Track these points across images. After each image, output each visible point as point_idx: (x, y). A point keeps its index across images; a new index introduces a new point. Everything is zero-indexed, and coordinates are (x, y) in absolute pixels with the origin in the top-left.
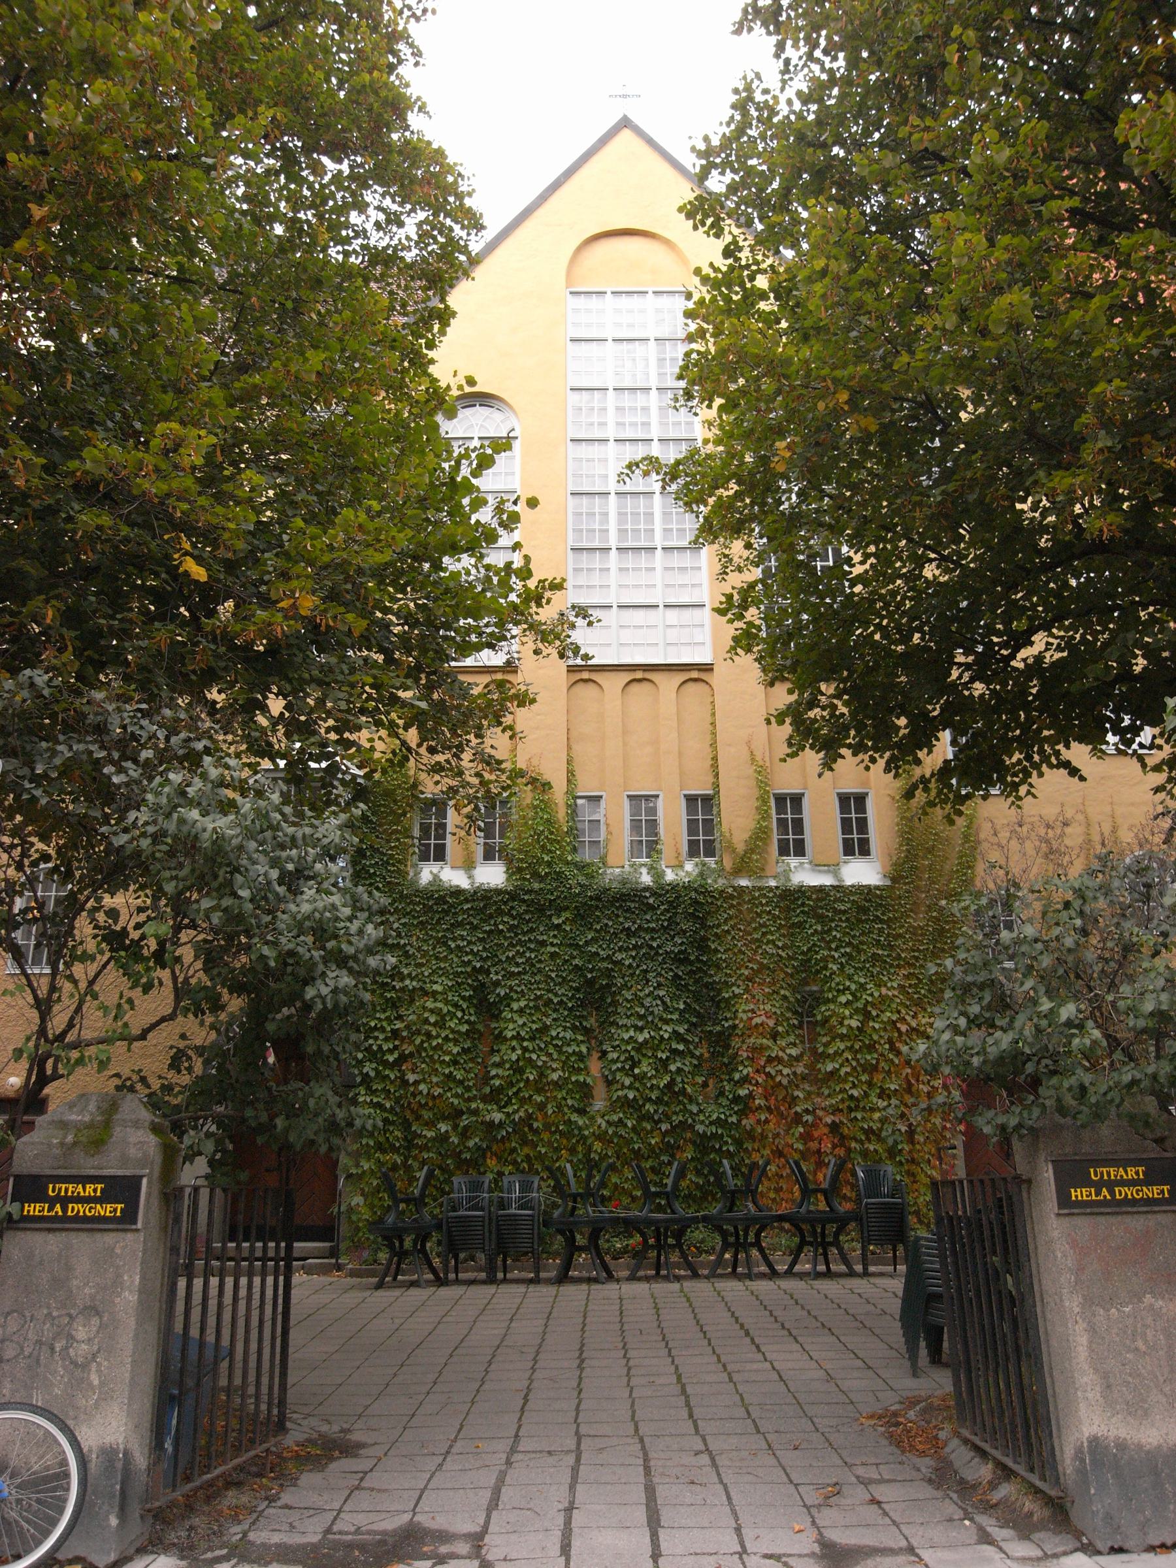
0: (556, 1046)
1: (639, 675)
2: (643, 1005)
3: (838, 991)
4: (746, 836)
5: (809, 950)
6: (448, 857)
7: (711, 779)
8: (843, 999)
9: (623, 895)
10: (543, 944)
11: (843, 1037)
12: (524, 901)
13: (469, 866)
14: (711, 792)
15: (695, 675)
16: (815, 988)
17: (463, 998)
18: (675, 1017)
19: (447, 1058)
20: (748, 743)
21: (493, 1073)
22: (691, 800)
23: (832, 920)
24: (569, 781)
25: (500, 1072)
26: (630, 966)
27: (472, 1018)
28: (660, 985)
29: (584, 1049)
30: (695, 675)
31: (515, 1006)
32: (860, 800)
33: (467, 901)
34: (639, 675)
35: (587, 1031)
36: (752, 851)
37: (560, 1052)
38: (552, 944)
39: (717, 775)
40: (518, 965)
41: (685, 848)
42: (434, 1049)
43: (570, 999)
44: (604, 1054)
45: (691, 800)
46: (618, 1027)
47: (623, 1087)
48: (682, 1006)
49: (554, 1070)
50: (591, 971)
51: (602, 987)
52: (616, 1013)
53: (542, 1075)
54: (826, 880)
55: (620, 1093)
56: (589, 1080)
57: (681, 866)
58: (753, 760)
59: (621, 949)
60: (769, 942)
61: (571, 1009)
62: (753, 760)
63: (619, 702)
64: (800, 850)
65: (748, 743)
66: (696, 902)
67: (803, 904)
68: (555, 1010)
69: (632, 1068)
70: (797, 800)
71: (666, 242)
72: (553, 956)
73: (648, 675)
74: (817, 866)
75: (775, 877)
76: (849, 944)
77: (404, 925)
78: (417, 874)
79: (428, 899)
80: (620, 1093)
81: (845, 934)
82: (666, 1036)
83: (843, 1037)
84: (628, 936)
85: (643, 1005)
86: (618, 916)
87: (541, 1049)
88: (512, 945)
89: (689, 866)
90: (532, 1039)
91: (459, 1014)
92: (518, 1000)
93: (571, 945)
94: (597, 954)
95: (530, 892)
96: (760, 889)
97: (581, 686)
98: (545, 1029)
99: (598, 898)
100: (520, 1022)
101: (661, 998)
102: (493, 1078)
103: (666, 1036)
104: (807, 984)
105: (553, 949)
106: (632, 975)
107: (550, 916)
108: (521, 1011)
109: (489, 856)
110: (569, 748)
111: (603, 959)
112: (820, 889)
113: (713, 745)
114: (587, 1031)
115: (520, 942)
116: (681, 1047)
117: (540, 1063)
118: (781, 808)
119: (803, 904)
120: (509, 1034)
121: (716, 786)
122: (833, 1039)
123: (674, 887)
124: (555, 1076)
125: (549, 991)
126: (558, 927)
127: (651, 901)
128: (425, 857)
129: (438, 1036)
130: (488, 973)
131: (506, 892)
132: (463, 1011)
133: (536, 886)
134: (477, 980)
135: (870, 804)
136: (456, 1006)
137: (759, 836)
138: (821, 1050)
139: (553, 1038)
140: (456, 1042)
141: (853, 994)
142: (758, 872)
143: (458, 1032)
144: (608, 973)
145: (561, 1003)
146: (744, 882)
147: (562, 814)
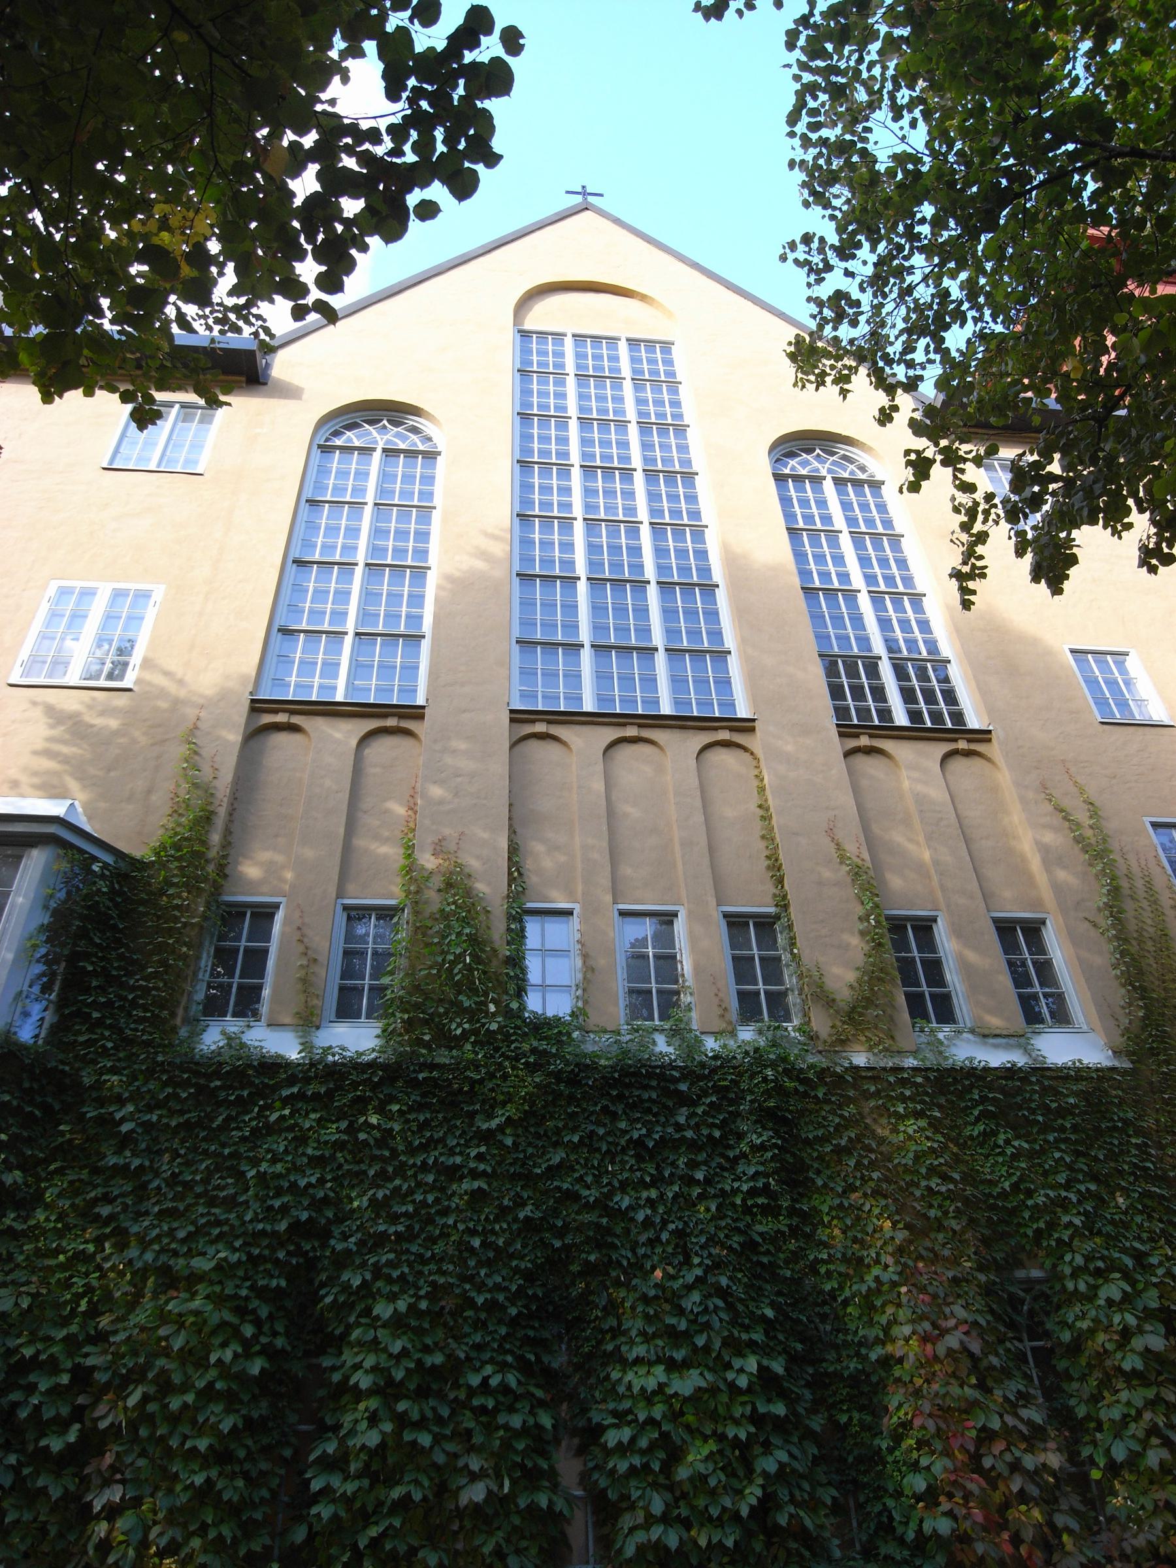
0: (483, 1409)
1: (631, 732)
2: (681, 1312)
3: (1098, 1273)
4: (851, 976)
5: (1015, 1187)
6: (264, 1009)
7: (770, 888)
8: (1113, 1290)
9: (625, 1072)
10: (453, 1173)
11: (1134, 1378)
12: (414, 1084)
13: (307, 1022)
14: (772, 910)
15: (724, 735)
16: (1036, 1273)
17: (261, 1293)
18: (758, 1336)
19: (203, 1444)
20: (830, 832)
21: (316, 1485)
22: (736, 923)
23: (1045, 1128)
24: (511, 880)
25: (336, 1481)
26: (647, 1223)
27: (280, 1342)
28: (718, 1265)
29: (546, 1421)
30: (724, 735)
31: (384, 1310)
32: (1034, 930)
33: (291, 1081)
34: (631, 732)
35: (549, 1377)
36: (869, 1002)
37: (490, 1428)
38: (475, 1175)
39: (780, 881)
40: (394, 1218)
41: (734, 1004)
42: (174, 1420)
43: (513, 1299)
44: (595, 1432)
45: (736, 923)
46: (625, 1364)
47: (650, 1521)
48: (769, 1313)
49: (474, 1477)
50: (561, 1233)
51: (589, 1270)
52: (616, 1332)
53: (442, 1490)
54: (1019, 1059)
55: (640, 1537)
56: (560, 1504)
57: (733, 1034)
58: (843, 859)
59: (624, 1186)
60: (932, 1171)
61: (514, 1322)
62: (843, 859)
63: (600, 767)
64: (946, 1013)
65: (830, 832)
66: (780, 1090)
67: (983, 1100)
68: (480, 1325)
69: (667, 1468)
70: (924, 928)
71: (643, 298)
72: (478, 1197)
73: (646, 733)
74: (985, 1035)
75: (915, 1053)
76: (1095, 1178)
77: (148, 1126)
78: (197, 1033)
79: (210, 1077)
80: (640, 1537)
81: (1078, 1154)
82: (743, 1382)
83: (1134, 1378)
84: (639, 1158)
85: (681, 1312)
86: (614, 1116)
87: (440, 1421)
88: (383, 1176)
89: (747, 1034)
90: (422, 1393)
91: (248, 1331)
92: (392, 1298)
93: (514, 1177)
94: (576, 1197)
95: (433, 1067)
96: (897, 1070)
97: (534, 744)
98: (454, 1369)
99: (573, 1080)
100: (397, 1347)
101: (723, 1293)
102: (315, 1498)
103: (743, 1382)
104: (1020, 1265)
105: (476, 1185)
106: (651, 1243)
107: (472, 1115)
108: (398, 1323)
109: (346, 1011)
110: (512, 831)
111: (588, 1207)
112: (1010, 1072)
113: (768, 837)
114: (549, 1377)
115: (401, 1170)
116: (780, 1409)
117: (440, 1458)
118: (901, 944)
119: (983, 1100)
120: (364, 1381)
121: (783, 904)
122: (1106, 1383)
123: (723, 1062)
124: (476, 1493)
125: (464, 1279)
126: (487, 1137)
127: (683, 1087)
128: (214, 1008)
129: (184, 1388)
130: (326, 1235)
131: (385, 1067)
132: (258, 1323)
133: (443, 1057)
134: (299, 1251)
135: (1052, 937)
136: (242, 1311)
137: (873, 977)
138: (1081, 1411)
139: (472, 1392)
140: (231, 1400)
141: (1126, 1276)
142: (886, 1042)
143: (242, 1378)
144: (601, 1239)
145: (492, 1306)
146: (860, 1059)
147: (498, 931)
